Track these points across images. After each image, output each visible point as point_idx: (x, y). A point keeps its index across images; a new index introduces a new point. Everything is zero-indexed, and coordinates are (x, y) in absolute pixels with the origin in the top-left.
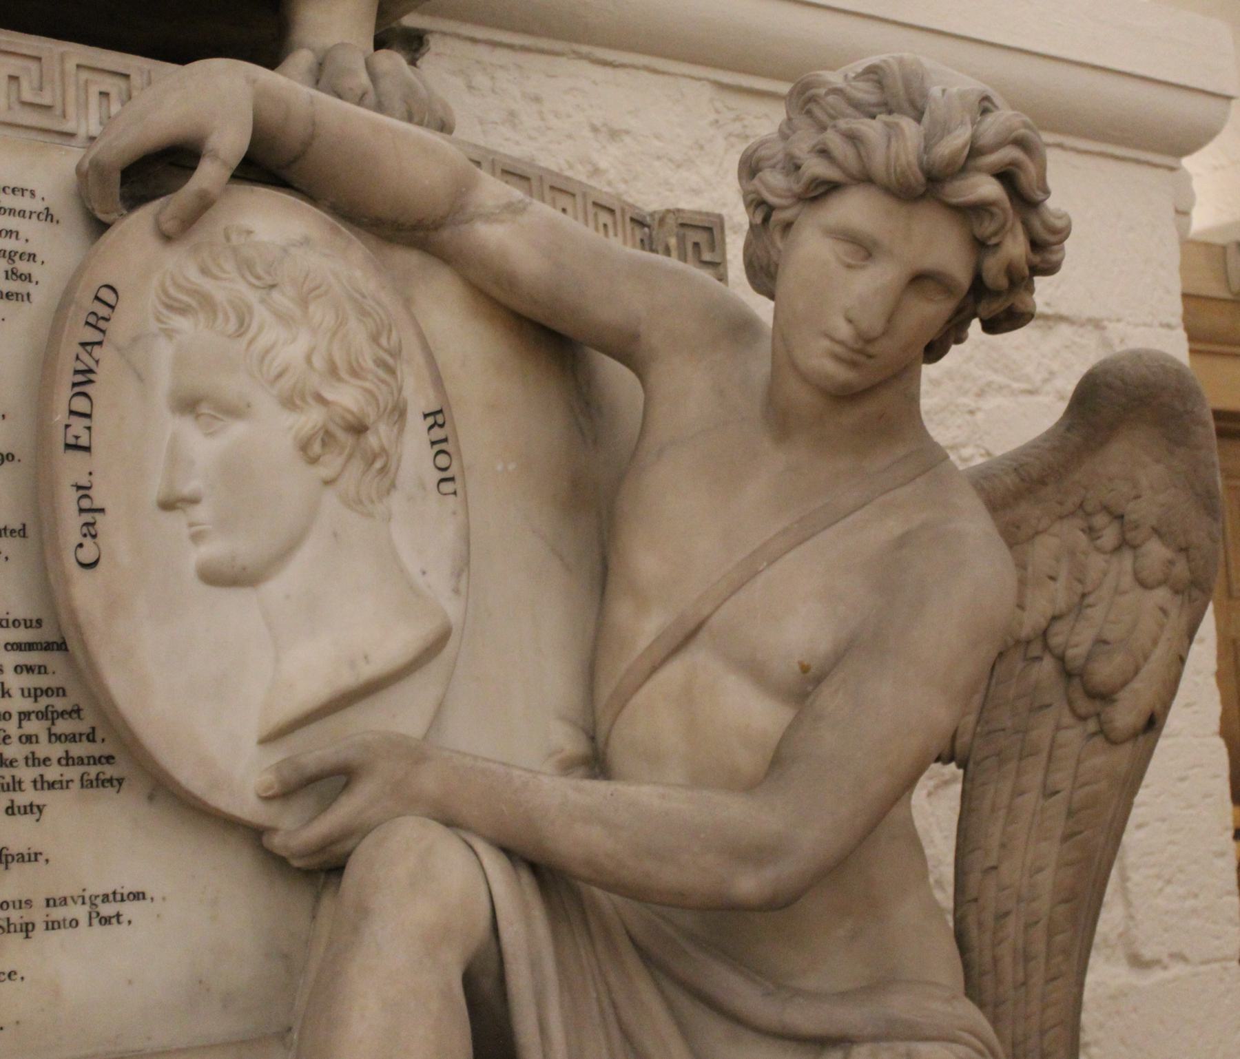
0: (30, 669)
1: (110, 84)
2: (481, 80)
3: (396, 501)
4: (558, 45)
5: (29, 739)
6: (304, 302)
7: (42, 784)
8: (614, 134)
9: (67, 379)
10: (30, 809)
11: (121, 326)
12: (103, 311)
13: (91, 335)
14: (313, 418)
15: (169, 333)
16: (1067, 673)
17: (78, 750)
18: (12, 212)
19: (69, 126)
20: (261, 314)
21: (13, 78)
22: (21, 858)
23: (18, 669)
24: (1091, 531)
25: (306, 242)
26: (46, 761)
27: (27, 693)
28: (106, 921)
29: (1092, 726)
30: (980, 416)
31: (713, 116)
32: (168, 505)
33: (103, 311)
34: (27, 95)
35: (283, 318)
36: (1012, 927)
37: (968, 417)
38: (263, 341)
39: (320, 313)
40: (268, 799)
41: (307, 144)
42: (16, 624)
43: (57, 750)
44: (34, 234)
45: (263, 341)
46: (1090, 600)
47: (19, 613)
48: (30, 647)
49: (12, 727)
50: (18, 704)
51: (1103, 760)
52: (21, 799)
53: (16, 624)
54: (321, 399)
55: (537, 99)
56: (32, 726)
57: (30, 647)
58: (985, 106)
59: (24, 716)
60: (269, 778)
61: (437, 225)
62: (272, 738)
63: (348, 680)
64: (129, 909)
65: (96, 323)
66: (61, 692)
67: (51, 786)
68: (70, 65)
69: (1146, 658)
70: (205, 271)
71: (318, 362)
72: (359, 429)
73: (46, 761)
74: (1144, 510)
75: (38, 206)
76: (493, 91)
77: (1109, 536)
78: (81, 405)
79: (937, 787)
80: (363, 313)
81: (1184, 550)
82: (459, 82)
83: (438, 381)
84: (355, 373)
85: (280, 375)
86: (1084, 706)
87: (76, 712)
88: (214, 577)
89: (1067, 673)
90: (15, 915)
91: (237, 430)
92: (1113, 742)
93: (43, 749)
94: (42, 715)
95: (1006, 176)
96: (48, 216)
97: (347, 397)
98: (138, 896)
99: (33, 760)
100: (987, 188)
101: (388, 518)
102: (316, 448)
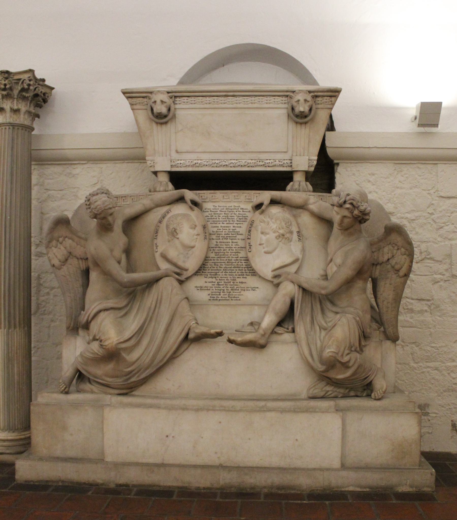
0: (245, 263)
1: (257, 195)
2: (349, 169)
3: (292, 243)
4: (362, 161)
5: (245, 270)
6: (276, 221)
7: (246, 275)
8: (373, 174)
9: (248, 231)
10: (246, 278)
11: (254, 225)
12: (252, 223)
13: (251, 226)
14: (277, 234)
15: (260, 225)
16: (393, 267)
17: (251, 271)
18: (245, 212)
19: (252, 201)
20: (270, 222)
21: (246, 196)
22: (244, 283)
23: (244, 263)
24: (393, 247)
25: (280, 212)
26: (247, 273)
27: (245, 265)
28: (253, 290)
29: (397, 275)
30: (451, 217)
31: (394, 168)
32: (260, 245)
33: (252, 223)
34: (247, 198)
35: (273, 223)
36: (385, 303)
37: (448, 217)
38: (270, 226)
39: (278, 222)
40: (273, 278)
41: (281, 200)
42: (244, 258)
43: (248, 271)
44: (248, 214)
45: (270, 226)
46: (395, 256)
47: (245, 256)
48: (246, 260)
49: (243, 269)
50: (244, 266)
51: (398, 280)
52: (244, 276)
53: (244, 258)
54: (278, 232)
55: (359, 171)
56: (246, 269)
57: (246, 260)
58: (348, 195)
59: (245, 268)
60: (272, 276)
61: (303, 206)
62: (273, 271)
63: (282, 264)
64: (256, 289)
65: (251, 225)
66: (249, 265)
67: (248, 275)
68: (253, 194)
69: (403, 265)
70: (264, 218)
71: (278, 228)
72: (283, 235)
73: (247, 273)
74: (400, 244)
75: (248, 210)
76: (351, 171)
77: (396, 248)
78: (249, 234)
79: (434, 283)
80: (284, 221)
81: (407, 250)
82: (345, 170)
83: (299, 227)
84: (283, 228)
85: (273, 229)
86: (396, 272)
87: (251, 267)
88: (266, 253)
89: (393, 267)
90: (243, 289)
91: (268, 236)
92: (401, 277)
93: (247, 271)
94: (247, 267)
95: (351, 204)
96: (249, 212)
97: (281, 231)
98: (257, 288)
99: (246, 272)
100: (348, 206)
101: (291, 245)
102: (278, 237)
